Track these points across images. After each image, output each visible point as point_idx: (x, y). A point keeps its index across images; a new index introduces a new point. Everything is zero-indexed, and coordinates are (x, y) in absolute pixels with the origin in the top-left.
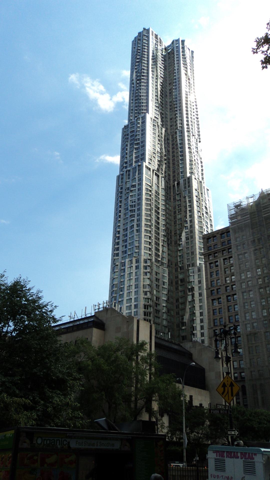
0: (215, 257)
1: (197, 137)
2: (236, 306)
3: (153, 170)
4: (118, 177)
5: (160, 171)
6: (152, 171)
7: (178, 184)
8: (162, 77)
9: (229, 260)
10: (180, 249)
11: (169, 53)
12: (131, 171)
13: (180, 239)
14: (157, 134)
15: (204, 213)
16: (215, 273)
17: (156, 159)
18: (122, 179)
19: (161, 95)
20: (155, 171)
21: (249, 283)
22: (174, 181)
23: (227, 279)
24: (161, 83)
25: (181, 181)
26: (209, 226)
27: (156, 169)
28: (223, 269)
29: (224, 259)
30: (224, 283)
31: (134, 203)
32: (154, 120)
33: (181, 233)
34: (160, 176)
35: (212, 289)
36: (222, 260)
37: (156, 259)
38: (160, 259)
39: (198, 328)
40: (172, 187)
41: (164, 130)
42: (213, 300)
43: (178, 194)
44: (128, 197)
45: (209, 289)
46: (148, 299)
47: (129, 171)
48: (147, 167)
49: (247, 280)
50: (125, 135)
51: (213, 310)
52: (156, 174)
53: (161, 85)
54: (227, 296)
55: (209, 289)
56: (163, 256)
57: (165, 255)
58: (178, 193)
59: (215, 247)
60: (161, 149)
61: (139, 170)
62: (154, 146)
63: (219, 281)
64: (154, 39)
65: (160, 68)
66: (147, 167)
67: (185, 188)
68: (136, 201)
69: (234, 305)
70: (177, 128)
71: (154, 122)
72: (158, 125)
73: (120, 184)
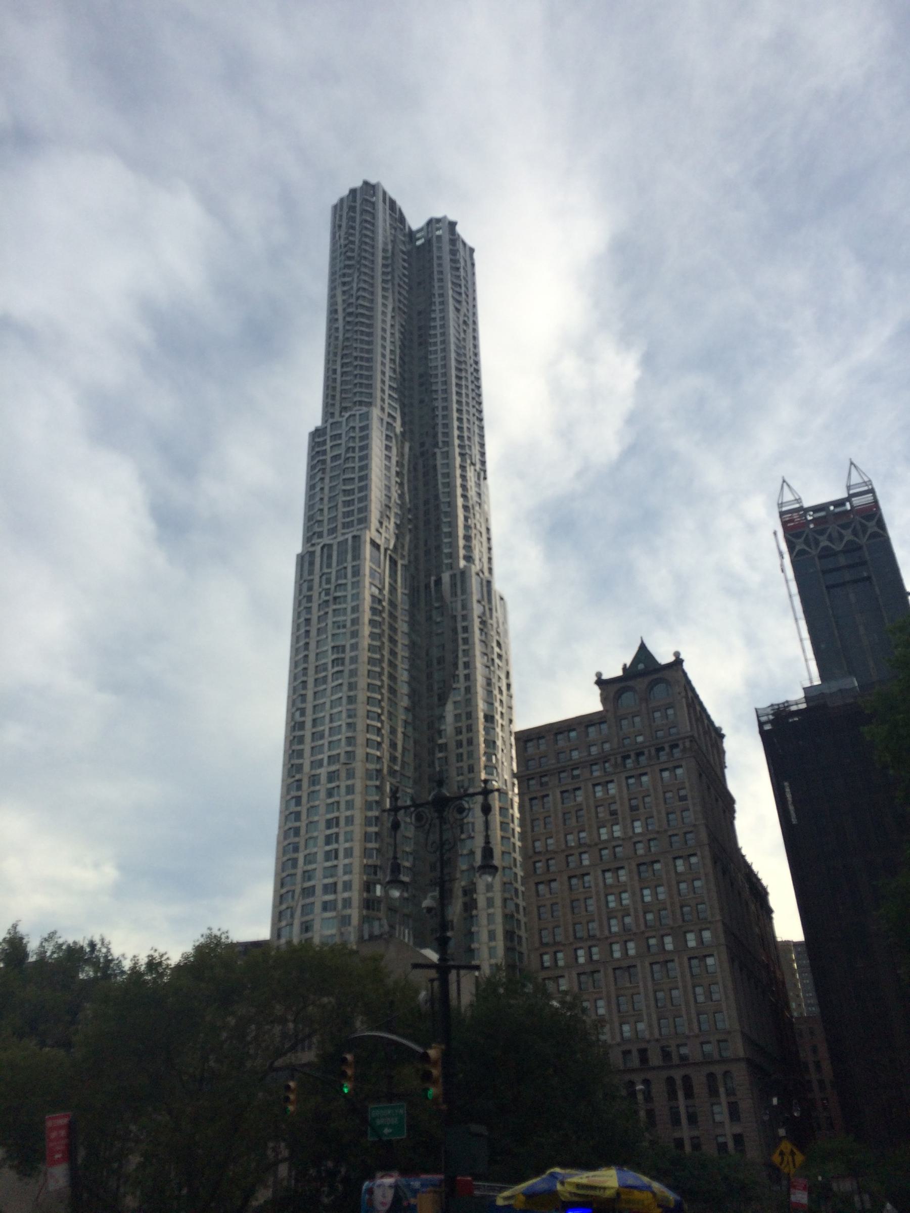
0: (542, 784)
1: (478, 466)
2: (590, 902)
3: (386, 550)
4: (301, 559)
5: (400, 551)
6: (382, 550)
7: (438, 582)
8: (404, 313)
9: (572, 796)
10: (440, 741)
11: (419, 247)
12: (335, 547)
13: (442, 717)
14: (394, 459)
15: (495, 656)
16: (542, 822)
17: (393, 520)
18: (312, 563)
19: (401, 358)
20: (389, 552)
21: (618, 849)
22: (428, 576)
23: (570, 837)
24: (402, 326)
25: (446, 577)
26: (504, 688)
27: (391, 547)
28: (560, 815)
29: (562, 792)
30: (563, 847)
32: (388, 423)
34: (400, 563)
35: (537, 859)
36: (558, 795)
37: (389, 767)
38: (397, 768)
39: (484, 936)
40: (422, 589)
42: (537, 884)
43: (437, 608)
44: (327, 613)
45: (530, 857)
46: (375, 867)
47: (330, 546)
48: (374, 543)
49: (614, 843)
50: (318, 452)
51: (539, 907)
52: (391, 557)
53: (402, 333)
54: (570, 878)
55: (530, 857)
56: (406, 759)
57: (410, 758)
58: (436, 605)
59: (543, 760)
60: (401, 496)
62: (388, 488)
63: (550, 841)
64: (388, 212)
65: (399, 285)
66: (374, 543)
67: (454, 594)
68: (349, 624)
69: (586, 899)
70: (436, 445)
71: (387, 429)
72: (396, 435)
73: (306, 576)
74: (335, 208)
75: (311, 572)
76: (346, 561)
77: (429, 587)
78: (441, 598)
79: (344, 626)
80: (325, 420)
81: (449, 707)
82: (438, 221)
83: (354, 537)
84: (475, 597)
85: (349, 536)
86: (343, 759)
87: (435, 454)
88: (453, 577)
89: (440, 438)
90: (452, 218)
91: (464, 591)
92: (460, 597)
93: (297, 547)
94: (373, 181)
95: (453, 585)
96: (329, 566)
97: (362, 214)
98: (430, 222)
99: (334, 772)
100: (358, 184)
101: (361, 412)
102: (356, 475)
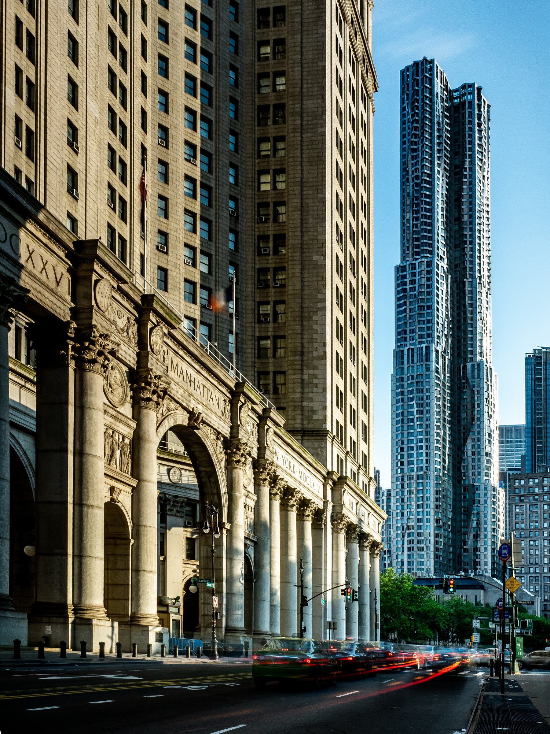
7: (465, 367)
12: (415, 351)
18: (402, 357)
25: (469, 365)
31: (421, 402)
33: (467, 439)
34: (447, 357)
41: (450, 276)
58: (464, 381)
60: (447, 315)
74: (402, 72)
75: (403, 363)
78: (466, 378)
79: (422, 399)
80: (403, 259)
81: (469, 441)
83: (426, 347)
84: (485, 380)
85: (424, 346)
86: (424, 470)
88: (473, 366)
89: (468, 272)
91: (479, 376)
93: (392, 346)
95: (473, 371)
96: (413, 362)
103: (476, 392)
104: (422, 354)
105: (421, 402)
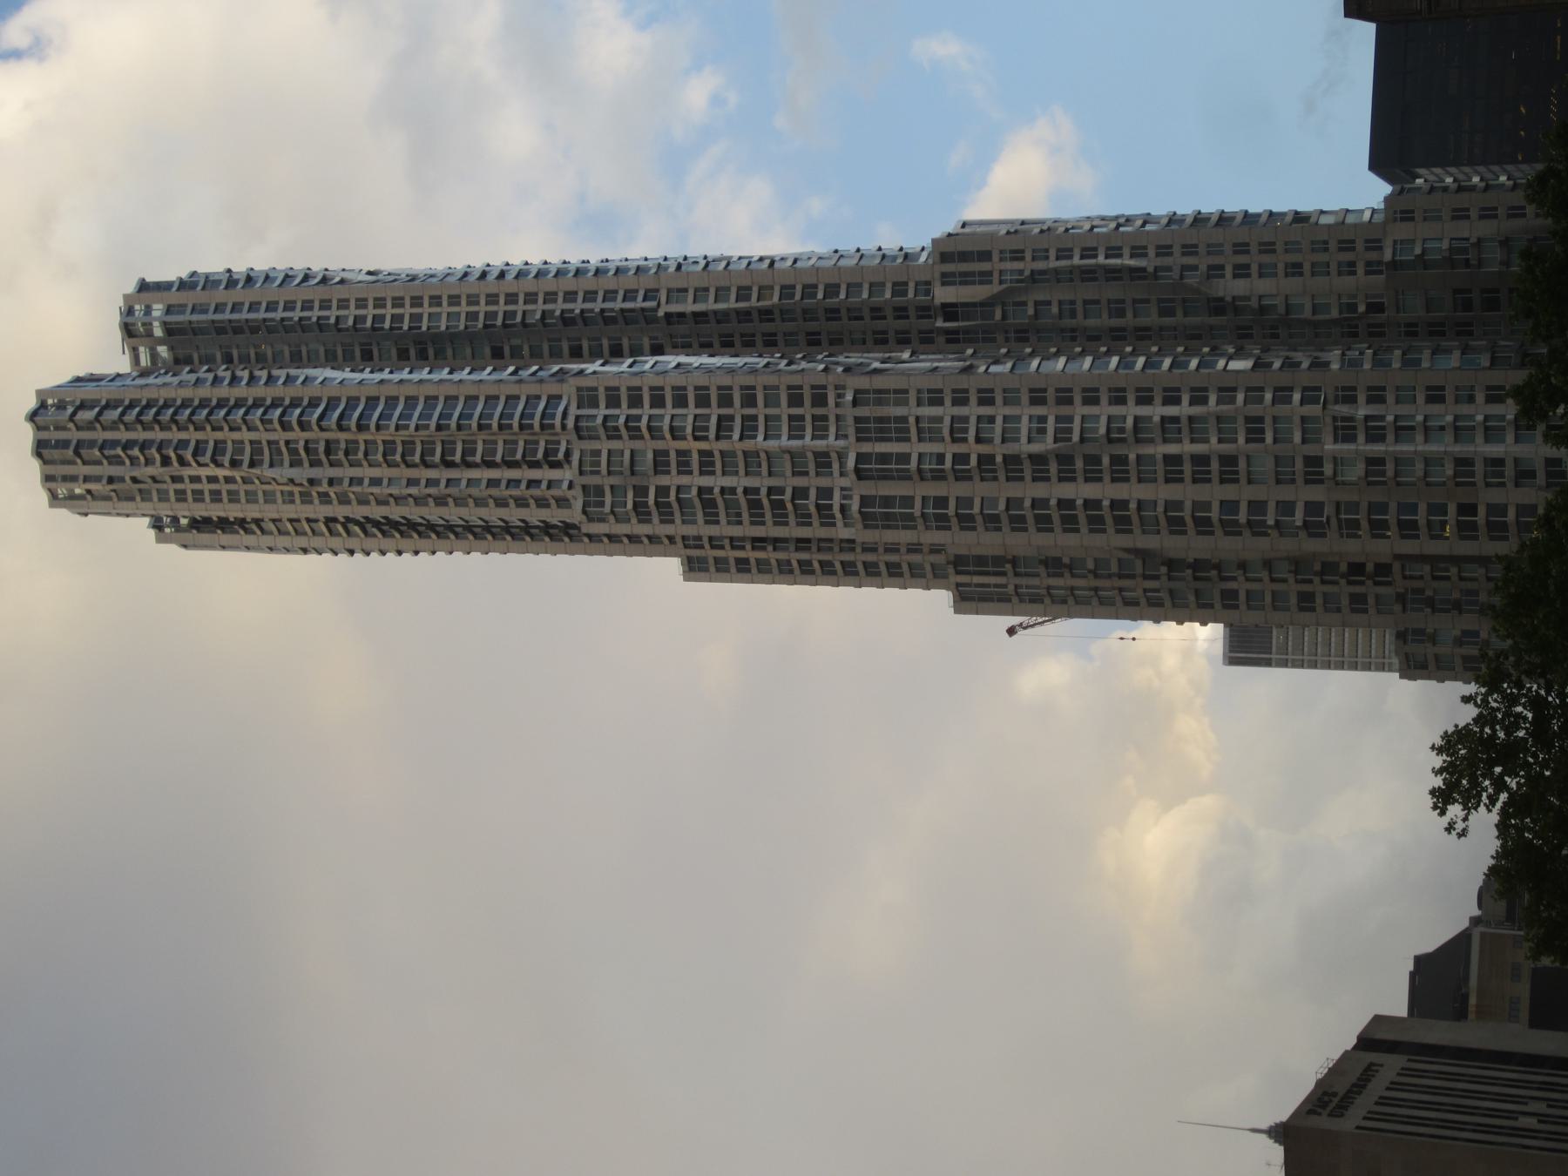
7: (950, 311)
12: (866, 448)
25: (943, 295)
31: (1051, 425)
58: (998, 315)
61: (879, 402)
67: (985, 278)
76: (904, 419)
77: (955, 331)
78: (988, 304)
79: (1042, 419)
82: (130, 311)
87: (668, 315)
88: (947, 279)
90: (131, 288)
92: (996, 265)
94: (32, 403)
95: (966, 279)
96: (905, 458)
97: (89, 445)
98: (128, 330)
99: (1336, 428)
100: (27, 434)
101: (574, 405)
102: (714, 412)
103: (1040, 265)
104: (881, 420)
105: (1051, 425)
